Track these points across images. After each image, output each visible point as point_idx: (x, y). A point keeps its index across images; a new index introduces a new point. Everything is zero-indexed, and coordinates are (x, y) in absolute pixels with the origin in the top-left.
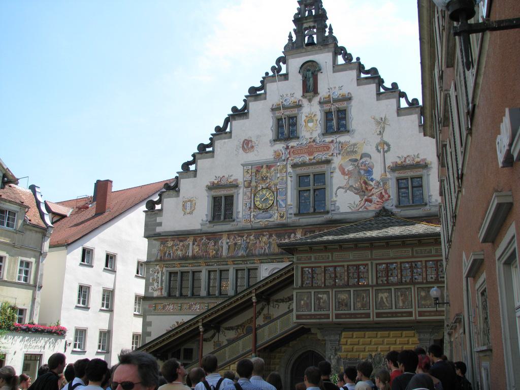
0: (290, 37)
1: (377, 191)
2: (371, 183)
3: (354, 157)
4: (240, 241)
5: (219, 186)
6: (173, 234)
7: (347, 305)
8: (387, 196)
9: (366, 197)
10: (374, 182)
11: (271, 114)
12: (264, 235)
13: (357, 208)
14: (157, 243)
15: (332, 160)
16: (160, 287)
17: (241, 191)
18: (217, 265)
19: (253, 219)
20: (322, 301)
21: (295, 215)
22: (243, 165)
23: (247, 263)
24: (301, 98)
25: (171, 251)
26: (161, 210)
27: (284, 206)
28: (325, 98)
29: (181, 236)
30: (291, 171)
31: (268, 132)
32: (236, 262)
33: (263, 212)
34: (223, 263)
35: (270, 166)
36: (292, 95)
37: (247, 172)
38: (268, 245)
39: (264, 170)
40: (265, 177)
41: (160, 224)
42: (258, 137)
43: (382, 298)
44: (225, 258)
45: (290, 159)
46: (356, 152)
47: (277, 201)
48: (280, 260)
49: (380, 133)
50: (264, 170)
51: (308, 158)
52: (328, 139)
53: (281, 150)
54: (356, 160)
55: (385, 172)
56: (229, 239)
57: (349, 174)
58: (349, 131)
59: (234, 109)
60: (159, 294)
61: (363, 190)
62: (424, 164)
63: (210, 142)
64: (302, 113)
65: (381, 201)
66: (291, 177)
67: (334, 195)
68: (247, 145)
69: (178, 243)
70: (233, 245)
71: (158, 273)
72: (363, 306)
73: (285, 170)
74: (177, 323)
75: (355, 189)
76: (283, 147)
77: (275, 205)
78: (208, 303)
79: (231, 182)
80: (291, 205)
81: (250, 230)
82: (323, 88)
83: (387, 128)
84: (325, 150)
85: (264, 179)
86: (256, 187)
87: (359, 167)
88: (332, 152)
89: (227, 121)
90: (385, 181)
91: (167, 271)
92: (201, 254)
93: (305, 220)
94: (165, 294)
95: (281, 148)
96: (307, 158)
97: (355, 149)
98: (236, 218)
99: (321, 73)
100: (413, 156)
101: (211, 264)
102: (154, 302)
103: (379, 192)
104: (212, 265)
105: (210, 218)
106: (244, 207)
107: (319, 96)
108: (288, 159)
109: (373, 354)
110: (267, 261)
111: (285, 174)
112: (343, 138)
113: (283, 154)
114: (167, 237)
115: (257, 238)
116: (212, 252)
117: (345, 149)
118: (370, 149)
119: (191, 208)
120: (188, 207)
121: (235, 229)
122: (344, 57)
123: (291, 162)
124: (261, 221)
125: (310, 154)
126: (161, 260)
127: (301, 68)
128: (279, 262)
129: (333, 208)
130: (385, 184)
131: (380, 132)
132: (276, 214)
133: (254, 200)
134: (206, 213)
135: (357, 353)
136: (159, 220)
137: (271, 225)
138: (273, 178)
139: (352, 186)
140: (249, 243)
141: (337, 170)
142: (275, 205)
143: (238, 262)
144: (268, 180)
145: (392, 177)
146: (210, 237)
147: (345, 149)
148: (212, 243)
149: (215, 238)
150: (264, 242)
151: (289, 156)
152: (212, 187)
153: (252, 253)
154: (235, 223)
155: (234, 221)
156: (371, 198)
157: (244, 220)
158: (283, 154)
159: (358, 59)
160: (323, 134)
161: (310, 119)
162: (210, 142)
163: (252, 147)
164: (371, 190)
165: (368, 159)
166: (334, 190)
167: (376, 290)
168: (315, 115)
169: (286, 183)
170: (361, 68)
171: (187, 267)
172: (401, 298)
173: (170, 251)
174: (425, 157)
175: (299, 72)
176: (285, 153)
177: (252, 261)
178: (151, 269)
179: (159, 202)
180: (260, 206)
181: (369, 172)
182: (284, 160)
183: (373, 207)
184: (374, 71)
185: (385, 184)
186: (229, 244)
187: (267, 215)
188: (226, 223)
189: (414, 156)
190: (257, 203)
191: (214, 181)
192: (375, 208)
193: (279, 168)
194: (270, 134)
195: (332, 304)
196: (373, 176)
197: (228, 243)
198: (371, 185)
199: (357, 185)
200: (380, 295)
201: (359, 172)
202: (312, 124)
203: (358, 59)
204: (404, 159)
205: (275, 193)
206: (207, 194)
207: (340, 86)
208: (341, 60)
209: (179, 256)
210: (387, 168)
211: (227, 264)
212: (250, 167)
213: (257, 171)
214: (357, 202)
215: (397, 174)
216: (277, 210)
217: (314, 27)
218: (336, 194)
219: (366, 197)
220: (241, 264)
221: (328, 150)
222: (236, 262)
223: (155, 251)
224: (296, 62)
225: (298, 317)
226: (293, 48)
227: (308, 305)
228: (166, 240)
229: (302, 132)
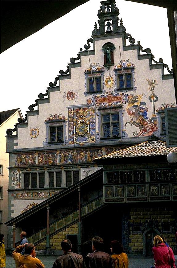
0: (96, 25)
1: (150, 125)
2: (146, 120)
4: (68, 155)
7: (134, 193)
8: (156, 128)
12: (82, 151)
13: (138, 135)
14: (15, 156)
15: (123, 105)
16: (18, 183)
17: (67, 124)
19: (75, 142)
20: (119, 191)
21: (101, 139)
23: (72, 168)
26: (16, 136)
27: (94, 133)
32: (66, 167)
35: (85, 108)
36: (98, 64)
37: (71, 112)
38: (85, 157)
39: (81, 111)
41: (17, 144)
42: (77, 90)
43: (153, 189)
47: (90, 130)
48: (93, 166)
49: (152, 90)
50: (81, 111)
52: (120, 93)
53: (91, 99)
54: (137, 106)
57: (133, 114)
58: (133, 88)
59: (61, 72)
60: (18, 187)
61: (141, 125)
63: (46, 92)
64: (104, 76)
66: (97, 116)
67: (124, 127)
68: (70, 95)
71: (17, 174)
72: (143, 194)
74: (30, 204)
75: (137, 123)
76: (93, 97)
77: (88, 132)
78: (49, 192)
79: (60, 118)
80: (99, 133)
82: (117, 62)
83: (156, 86)
84: (118, 100)
86: (77, 122)
87: (139, 110)
88: (123, 101)
89: (57, 79)
90: (154, 119)
94: (22, 186)
95: (92, 98)
96: (107, 104)
99: (116, 51)
100: (171, 104)
101: (50, 168)
102: (15, 192)
103: (151, 126)
104: (51, 169)
107: (114, 66)
109: (149, 220)
111: (94, 114)
112: (129, 93)
113: (92, 101)
115: (78, 153)
116: (51, 161)
119: (36, 134)
120: (35, 133)
122: (130, 41)
123: (98, 106)
124: (80, 143)
125: (110, 101)
127: (103, 47)
128: (92, 167)
131: (152, 89)
132: (89, 138)
134: (46, 137)
135: (139, 220)
136: (15, 141)
139: (134, 122)
140: (73, 155)
142: (88, 132)
148: (50, 156)
151: (96, 103)
152: (48, 122)
153: (75, 162)
154: (64, 143)
155: (63, 142)
156: (146, 129)
158: (92, 101)
159: (139, 42)
160: (117, 90)
162: (46, 92)
163: (73, 96)
170: (139, 47)
171: (36, 170)
172: (163, 190)
175: (102, 50)
176: (94, 101)
178: (12, 172)
179: (15, 130)
181: (145, 113)
182: (93, 105)
183: (147, 135)
184: (148, 50)
185: (154, 121)
189: (172, 104)
191: (50, 117)
194: (84, 89)
195: (125, 193)
198: (146, 122)
199: (138, 121)
200: (152, 188)
201: (139, 114)
202: (110, 83)
203: (139, 42)
204: (166, 106)
205: (88, 125)
206: (46, 126)
207: (128, 60)
208: (128, 43)
210: (155, 111)
211: (60, 169)
212: (73, 109)
213: (77, 111)
214: (138, 132)
216: (90, 136)
217: (110, 20)
218: (125, 127)
220: (69, 168)
221: (120, 100)
223: (14, 161)
224: (100, 44)
225: (106, 200)
226: (98, 34)
227: (112, 194)
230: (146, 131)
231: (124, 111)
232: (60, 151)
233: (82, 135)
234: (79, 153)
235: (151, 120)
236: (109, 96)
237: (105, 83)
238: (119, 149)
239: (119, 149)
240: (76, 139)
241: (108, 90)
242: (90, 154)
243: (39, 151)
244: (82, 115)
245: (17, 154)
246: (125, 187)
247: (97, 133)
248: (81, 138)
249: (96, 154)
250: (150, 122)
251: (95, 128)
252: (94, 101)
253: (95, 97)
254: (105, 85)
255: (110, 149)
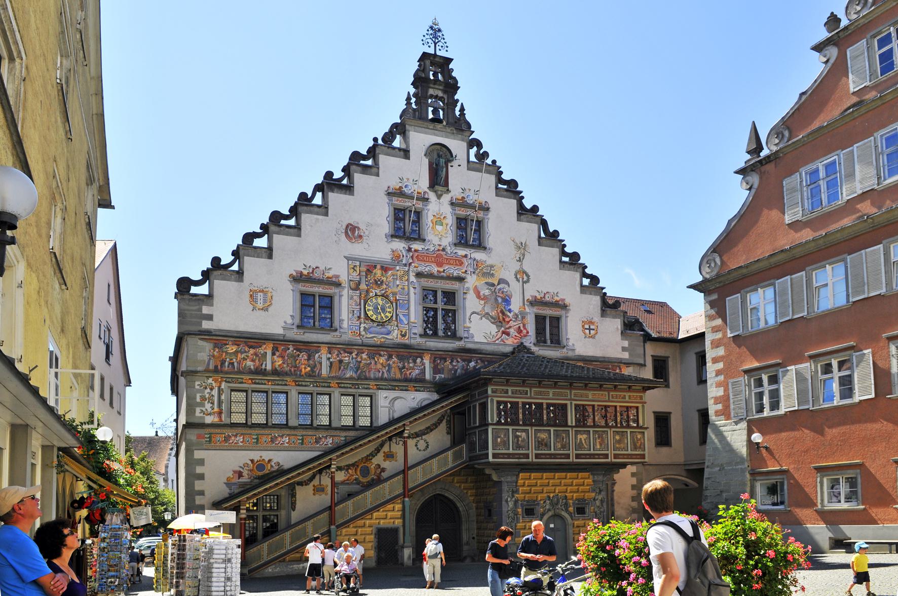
1: (515, 324)
2: (509, 314)
3: (490, 281)
4: (347, 359)
5: (310, 278)
6: (235, 335)
8: (525, 331)
9: (503, 329)
10: (512, 313)
11: (386, 199)
12: (380, 355)
13: (494, 340)
17: (345, 292)
18: (314, 386)
19: (363, 333)
21: (421, 336)
22: (348, 259)
23: (359, 388)
24: (428, 190)
25: (234, 360)
26: (209, 298)
27: (406, 323)
28: (458, 200)
29: (253, 340)
30: (415, 281)
31: (383, 222)
32: (342, 385)
33: (378, 325)
34: (324, 384)
35: (386, 268)
37: (354, 269)
38: (387, 368)
39: (378, 272)
40: (379, 281)
42: (369, 225)
44: (323, 378)
45: (413, 264)
46: (493, 275)
47: (397, 315)
48: (404, 388)
50: (378, 272)
51: (436, 269)
52: (461, 252)
54: (493, 285)
55: (524, 305)
56: (330, 353)
57: (485, 298)
58: (485, 248)
61: (500, 320)
62: (563, 304)
65: (519, 335)
67: (467, 320)
68: (352, 232)
69: (247, 349)
70: (337, 362)
73: (406, 277)
75: (492, 317)
76: (404, 248)
77: (394, 319)
81: (360, 345)
83: (527, 256)
84: (457, 265)
85: (378, 283)
86: (367, 291)
87: (496, 293)
88: (465, 269)
91: (229, 387)
92: (287, 369)
93: (433, 344)
95: (402, 249)
96: (435, 269)
97: (492, 272)
98: (338, 327)
101: (304, 383)
103: (517, 326)
104: (305, 386)
105: (297, 321)
106: (350, 315)
108: (410, 264)
110: (387, 388)
111: (407, 282)
112: (479, 255)
114: (225, 339)
115: (371, 356)
116: (305, 368)
117: (481, 268)
118: (509, 276)
121: (338, 342)
125: (440, 264)
126: (216, 371)
129: (466, 335)
130: (523, 318)
131: (520, 258)
132: (396, 331)
133: (365, 308)
137: (388, 344)
138: (391, 284)
139: (488, 314)
140: (360, 362)
141: (471, 292)
142: (394, 319)
143: (346, 385)
144: (384, 286)
145: (531, 313)
146: (302, 347)
147: (481, 268)
148: (303, 356)
149: (309, 351)
150: (382, 364)
151: (411, 261)
154: (337, 333)
155: (336, 330)
157: (350, 332)
160: (455, 245)
161: (439, 221)
163: (360, 237)
164: (508, 322)
165: (506, 286)
166: (468, 314)
167: (613, 431)
168: (445, 217)
169: (408, 294)
171: (265, 384)
173: (231, 359)
174: (564, 298)
176: (407, 256)
177: (366, 386)
178: (197, 383)
180: (374, 318)
181: (507, 301)
182: (405, 265)
186: (331, 360)
187: (383, 330)
188: (323, 332)
190: (370, 313)
192: (513, 343)
193: (399, 273)
194: (385, 227)
196: (511, 307)
197: (329, 359)
199: (493, 313)
201: (496, 300)
204: (542, 295)
205: (394, 304)
209: (250, 369)
211: (329, 387)
212: (358, 263)
213: (368, 270)
214: (494, 333)
215: (535, 310)
216: (397, 326)
218: (469, 319)
219: (503, 329)
220: (350, 388)
222: (342, 385)
228: (224, 342)
229: (429, 235)
230: (508, 334)
231: (468, 289)
232: (328, 347)
233: (379, 322)
234: (374, 359)
235: (516, 314)
236: (438, 253)
237: (431, 225)
238: (459, 360)
239: (459, 360)
240: (365, 327)
241: (436, 241)
242: (399, 364)
243: (278, 343)
244: (379, 281)
245: (212, 341)
246: (532, 430)
247: (413, 323)
248: (378, 327)
249: (411, 365)
250: (516, 319)
251: (409, 313)
252: (407, 256)
253: (409, 250)
254: (430, 228)
255: (441, 359)
